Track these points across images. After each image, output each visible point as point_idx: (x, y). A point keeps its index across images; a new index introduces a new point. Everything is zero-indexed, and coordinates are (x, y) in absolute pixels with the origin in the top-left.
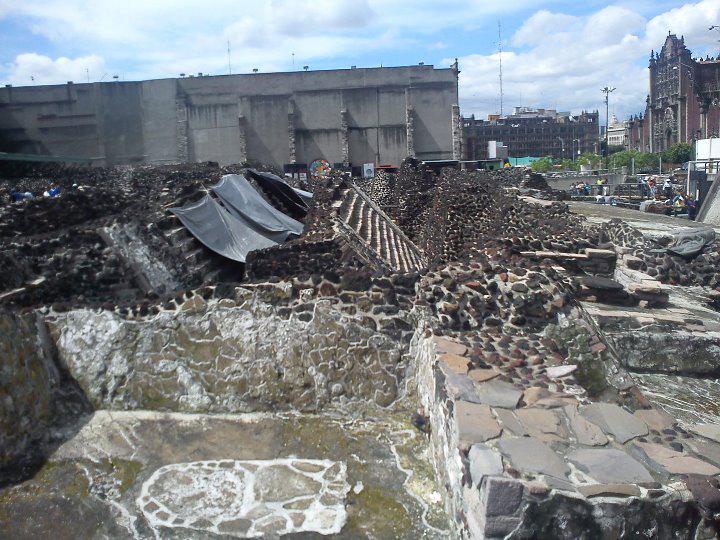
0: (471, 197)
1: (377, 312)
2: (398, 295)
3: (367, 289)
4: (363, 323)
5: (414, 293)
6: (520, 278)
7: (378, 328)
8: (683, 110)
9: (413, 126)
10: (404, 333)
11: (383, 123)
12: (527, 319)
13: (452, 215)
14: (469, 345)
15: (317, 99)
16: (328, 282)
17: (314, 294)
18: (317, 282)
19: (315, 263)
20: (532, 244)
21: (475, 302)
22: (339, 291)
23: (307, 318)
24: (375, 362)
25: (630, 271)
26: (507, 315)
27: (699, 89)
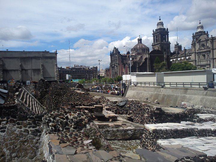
0: (61, 91)
1: (29, 128)
2: (37, 122)
3: (26, 120)
4: (25, 132)
5: (42, 121)
6: (75, 114)
7: (30, 133)
8: (119, 67)
9: (43, 69)
10: (39, 134)
11: (34, 68)
12: (77, 127)
13: (55, 97)
14: (59, 136)
15: (11, 60)
16: (12, 118)
17: (7, 123)
18: (8, 119)
19: (8, 113)
20: (79, 104)
21: (61, 122)
22: (16, 121)
23: (4, 131)
24: (28, 145)
25: (107, 111)
26: (71, 126)
27: (122, 62)
